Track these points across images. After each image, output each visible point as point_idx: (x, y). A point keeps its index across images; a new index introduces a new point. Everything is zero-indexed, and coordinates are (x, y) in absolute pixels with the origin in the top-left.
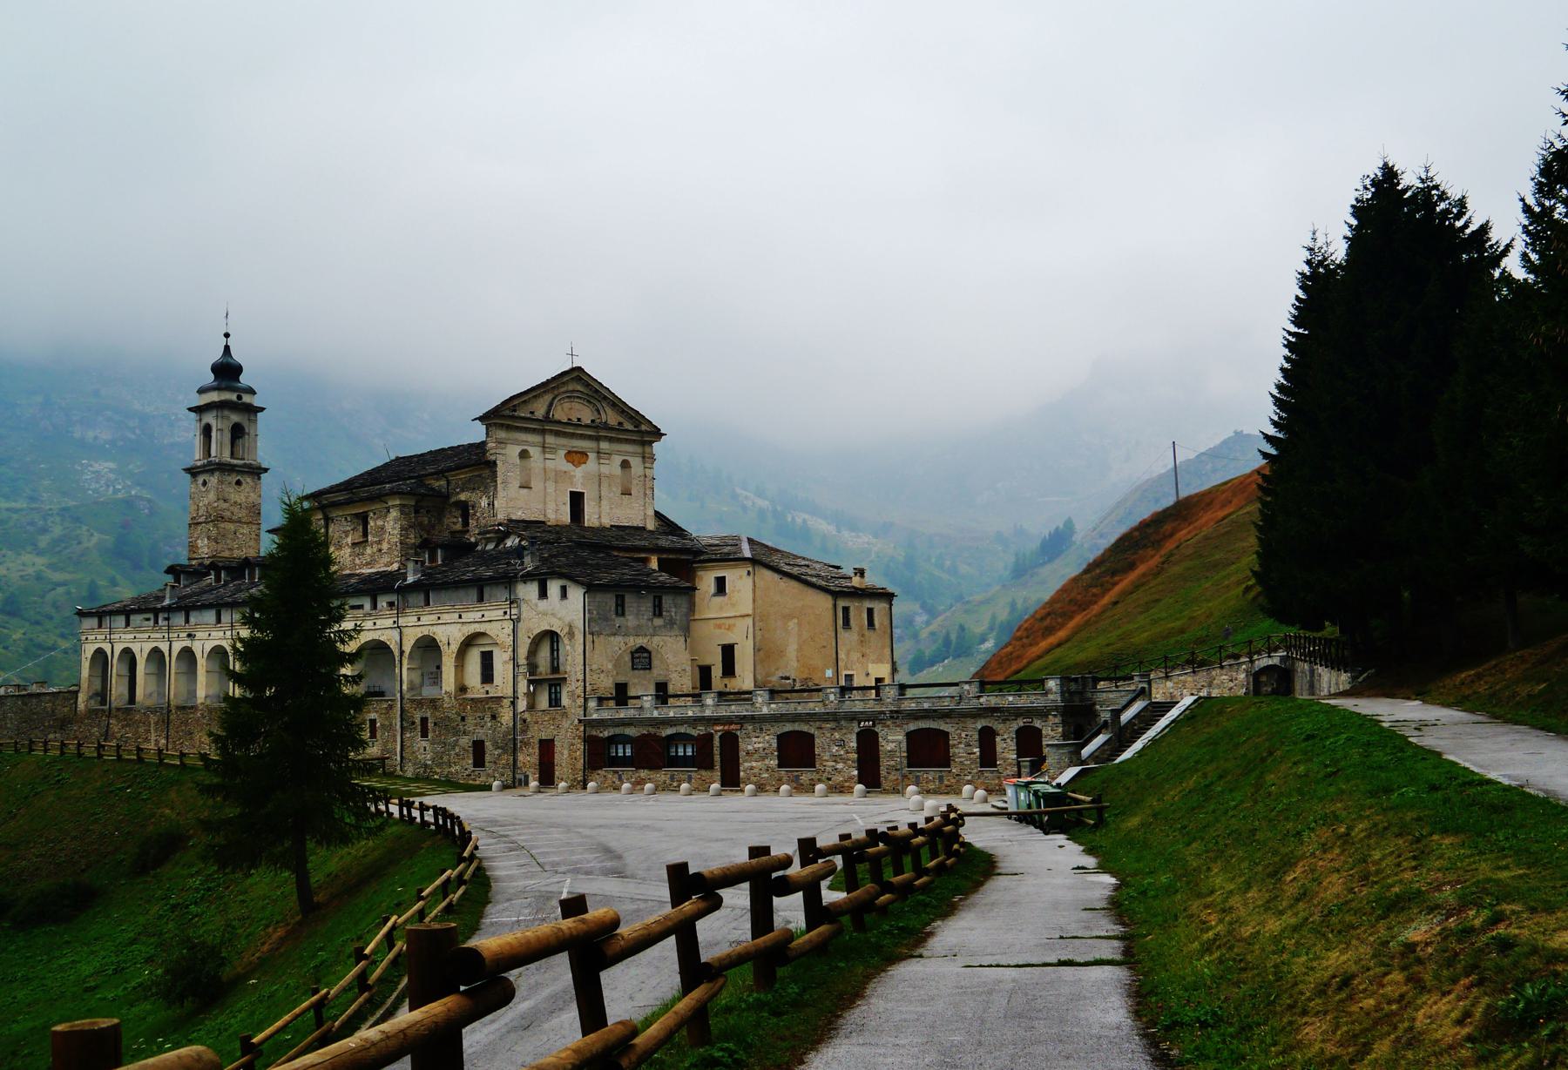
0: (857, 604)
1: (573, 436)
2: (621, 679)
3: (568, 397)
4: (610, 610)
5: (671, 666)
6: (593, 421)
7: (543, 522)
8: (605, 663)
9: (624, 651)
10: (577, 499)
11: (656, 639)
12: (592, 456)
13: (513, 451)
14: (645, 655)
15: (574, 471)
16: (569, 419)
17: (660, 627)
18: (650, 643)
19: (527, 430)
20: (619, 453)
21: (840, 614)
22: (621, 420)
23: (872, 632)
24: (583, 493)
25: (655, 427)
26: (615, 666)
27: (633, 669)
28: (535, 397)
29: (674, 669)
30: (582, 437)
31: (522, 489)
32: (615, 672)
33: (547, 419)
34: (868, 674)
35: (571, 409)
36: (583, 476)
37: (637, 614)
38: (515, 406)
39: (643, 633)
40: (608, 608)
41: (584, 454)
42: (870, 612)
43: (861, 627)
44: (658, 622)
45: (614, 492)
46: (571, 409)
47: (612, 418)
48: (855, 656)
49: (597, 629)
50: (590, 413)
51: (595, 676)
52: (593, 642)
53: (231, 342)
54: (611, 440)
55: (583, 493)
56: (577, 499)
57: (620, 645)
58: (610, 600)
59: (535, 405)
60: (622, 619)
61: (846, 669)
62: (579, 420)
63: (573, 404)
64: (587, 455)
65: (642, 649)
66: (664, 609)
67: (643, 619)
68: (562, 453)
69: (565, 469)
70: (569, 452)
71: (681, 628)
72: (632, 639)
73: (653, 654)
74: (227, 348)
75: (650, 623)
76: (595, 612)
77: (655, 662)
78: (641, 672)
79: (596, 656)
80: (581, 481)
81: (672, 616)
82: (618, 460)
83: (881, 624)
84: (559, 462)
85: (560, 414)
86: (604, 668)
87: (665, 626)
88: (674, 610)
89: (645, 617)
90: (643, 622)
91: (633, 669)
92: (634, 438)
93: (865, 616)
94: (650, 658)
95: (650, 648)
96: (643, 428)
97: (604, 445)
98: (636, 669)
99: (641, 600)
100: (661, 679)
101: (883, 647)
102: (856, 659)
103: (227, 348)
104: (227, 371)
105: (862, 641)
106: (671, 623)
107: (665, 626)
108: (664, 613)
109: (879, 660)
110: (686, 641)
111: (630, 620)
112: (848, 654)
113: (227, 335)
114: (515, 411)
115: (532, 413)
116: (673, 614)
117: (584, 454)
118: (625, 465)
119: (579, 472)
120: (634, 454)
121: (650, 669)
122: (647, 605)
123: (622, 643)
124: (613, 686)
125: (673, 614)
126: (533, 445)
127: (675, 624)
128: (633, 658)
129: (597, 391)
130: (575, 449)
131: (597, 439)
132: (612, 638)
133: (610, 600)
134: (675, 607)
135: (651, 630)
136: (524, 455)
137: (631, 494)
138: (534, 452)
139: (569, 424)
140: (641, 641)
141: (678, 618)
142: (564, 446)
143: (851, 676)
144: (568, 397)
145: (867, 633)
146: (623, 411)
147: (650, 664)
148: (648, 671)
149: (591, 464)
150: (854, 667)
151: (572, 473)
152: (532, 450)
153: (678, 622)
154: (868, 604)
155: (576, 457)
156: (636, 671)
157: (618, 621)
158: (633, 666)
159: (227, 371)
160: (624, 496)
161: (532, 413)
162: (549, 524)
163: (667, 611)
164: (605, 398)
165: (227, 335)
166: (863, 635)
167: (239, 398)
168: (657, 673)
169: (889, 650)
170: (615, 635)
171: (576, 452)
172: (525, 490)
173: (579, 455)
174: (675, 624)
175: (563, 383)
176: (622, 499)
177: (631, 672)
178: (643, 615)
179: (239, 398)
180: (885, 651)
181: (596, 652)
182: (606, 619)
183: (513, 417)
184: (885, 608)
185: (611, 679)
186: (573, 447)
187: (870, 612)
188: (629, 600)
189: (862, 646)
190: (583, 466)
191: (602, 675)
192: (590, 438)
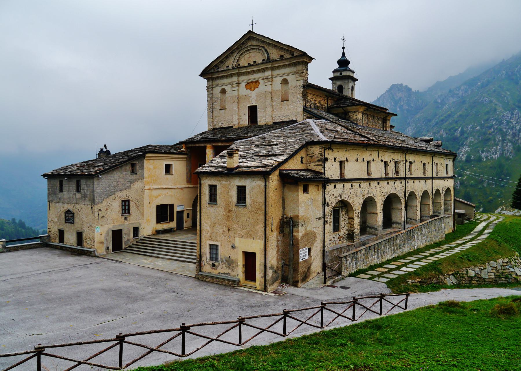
0: (224, 183)
1: (249, 73)
2: (61, 228)
3: (246, 51)
4: (56, 189)
5: (84, 223)
6: (263, 60)
7: (232, 127)
8: (54, 217)
9: (62, 212)
10: (253, 111)
11: (77, 206)
12: (261, 82)
13: (217, 91)
14: (71, 215)
15: (251, 94)
16: (249, 64)
17: (79, 199)
18: (74, 208)
19: (222, 77)
20: (279, 76)
21: (206, 191)
22: (282, 53)
23: (240, 209)
24: (257, 106)
25: (302, 51)
26: (58, 220)
27: (66, 222)
28: (227, 57)
29: (86, 225)
30: (254, 72)
31: (221, 110)
32: (58, 224)
33: (239, 67)
34: (233, 247)
35: (249, 57)
36: (256, 96)
37: (68, 191)
38: (216, 66)
39: (71, 202)
40: (56, 187)
41: (257, 82)
42: (241, 190)
43: (228, 204)
44: (78, 195)
45: (276, 101)
46: (249, 57)
47: (275, 54)
48: (220, 229)
49: (51, 199)
50: (261, 56)
51: (51, 224)
52: (49, 205)
53: (345, 50)
54: (272, 69)
55: (257, 106)
56: (253, 111)
57: (62, 208)
58: (56, 183)
59: (229, 61)
60: (61, 193)
61: (211, 239)
62: (255, 62)
63: (250, 54)
64: (259, 82)
65: (68, 212)
66: (81, 188)
67: (71, 194)
68: (244, 84)
69: (244, 94)
70: (248, 83)
71: (89, 200)
72: (66, 205)
73: (75, 214)
74: (344, 53)
75: (74, 196)
76: (50, 190)
77: (76, 220)
78: (70, 224)
79: (50, 214)
80: (255, 98)
81: (85, 192)
82: (278, 81)
83: (253, 202)
84: (243, 90)
85: (243, 62)
86: (54, 220)
87: (81, 198)
88: (86, 188)
89: (72, 193)
90: (71, 195)
91: (66, 222)
92: (286, 63)
93: (234, 194)
94: (73, 217)
95: (74, 211)
96: (295, 54)
97: (268, 73)
98: (67, 223)
99: (70, 183)
100: (79, 230)
101: (255, 224)
102: (221, 232)
103: (344, 53)
104: (344, 63)
105: (228, 216)
106: (85, 197)
107: (81, 198)
108: (81, 190)
109: (250, 235)
110: (92, 208)
111: (65, 195)
112: (213, 226)
113: (343, 48)
114: (219, 68)
115: (228, 67)
116: (86, 191)
117: (257, 82)
118: (285, 82)
119: (253, 94)
120: (289, 74)
121: (73, 223)
122: (73, 185)
123: (62, 208)
124: (57, 231)
125: (86, 191)
126: (227, 85)
127: (87, 197)
128: (65, 216)
129: (264, 42)
130: (250, 81)
131: (263, 70)
132: (58, 204)
133: (56, 183)
134: (87, 187)
135: (75, 201)
136: (223, 91)
137: (287, 100)
138: (228, 88)
139: (250, 65)
140: (70, 207)
141: (88, 193)
142: (244, 80)
143: (217, 246)
144: (246, 51)
145: (234, 209)
146: (282, 48)
147: (73, 220)
148: (73, 224)
149: (263, 87)
150: (219, 239)
151: (249, 96)
152: (226, 88)
153: (88, 196)
154: (238, 182)
155: (252, 85)
156: (67, 224)
157: (60, 195)
158: (65, 221)
159: (344, 63)
160: (283, 103)
161: (228, 67)
162: (234, 127)
163: (83, 189)
164: (269, 44)
165: (343, 48)
166: (230, 211)
167: (341, 74)
168: (77, 226)
169: (263, 226)
170: (58, 202)
171: (253, 82)
172: (223, 111)
173: (254, 84)
174: (87, 197)
175: (243, 43)
176: (281, 105)
177: (65, 224)
178: (71, 192)
179: (341, 74)
180: (257, 227)
181: (51, 211)
182: (55, 194)
183: (218, 72)
184: (259, 186)
185: (57, 227)
186: (249, 80)
187: (241, 190)
188: (65, 183)
189: (228, 221)
190: (256, 89)
191: (53, 224)
192: (259, 71)
